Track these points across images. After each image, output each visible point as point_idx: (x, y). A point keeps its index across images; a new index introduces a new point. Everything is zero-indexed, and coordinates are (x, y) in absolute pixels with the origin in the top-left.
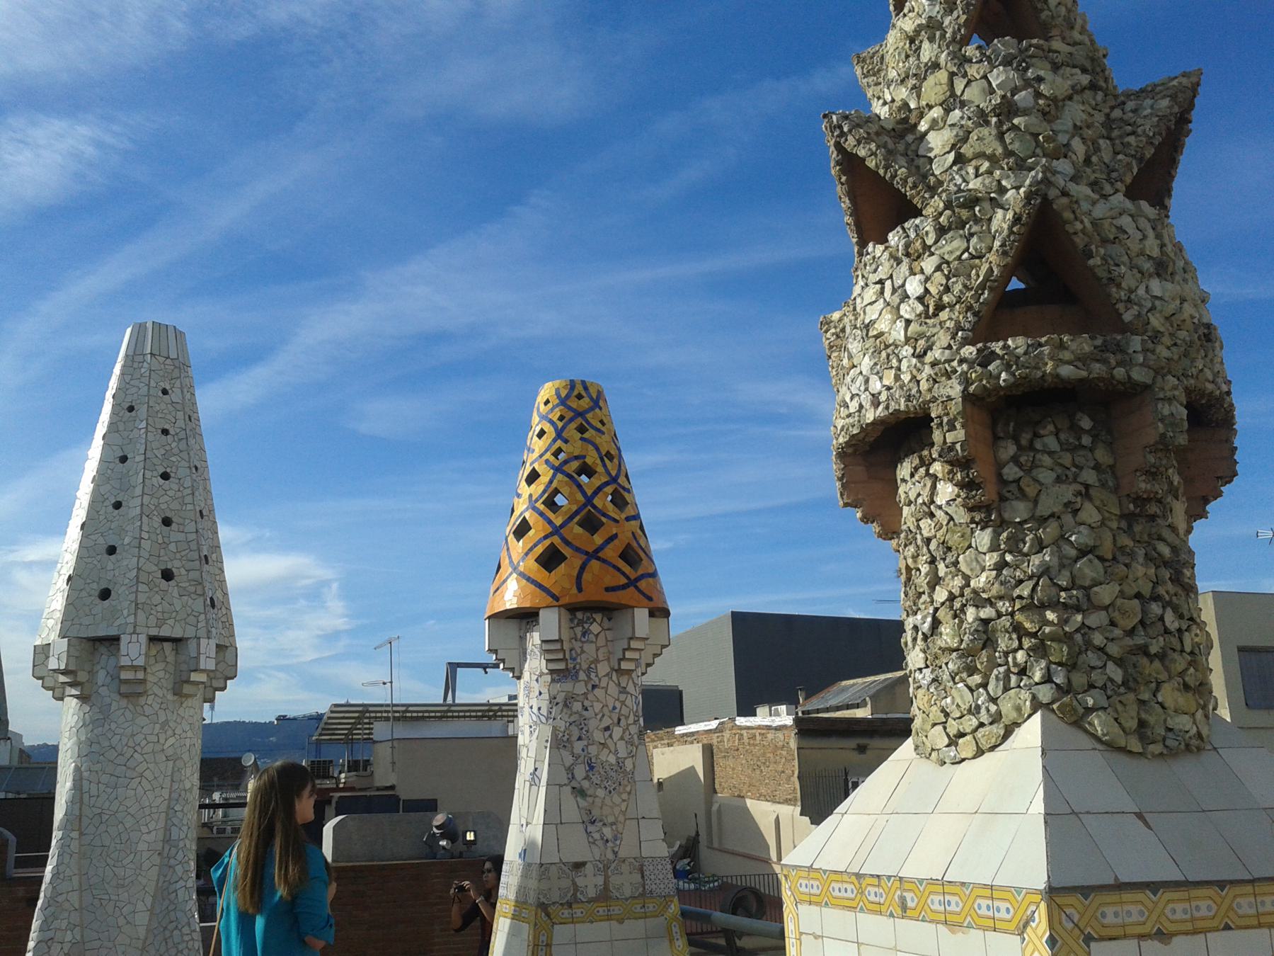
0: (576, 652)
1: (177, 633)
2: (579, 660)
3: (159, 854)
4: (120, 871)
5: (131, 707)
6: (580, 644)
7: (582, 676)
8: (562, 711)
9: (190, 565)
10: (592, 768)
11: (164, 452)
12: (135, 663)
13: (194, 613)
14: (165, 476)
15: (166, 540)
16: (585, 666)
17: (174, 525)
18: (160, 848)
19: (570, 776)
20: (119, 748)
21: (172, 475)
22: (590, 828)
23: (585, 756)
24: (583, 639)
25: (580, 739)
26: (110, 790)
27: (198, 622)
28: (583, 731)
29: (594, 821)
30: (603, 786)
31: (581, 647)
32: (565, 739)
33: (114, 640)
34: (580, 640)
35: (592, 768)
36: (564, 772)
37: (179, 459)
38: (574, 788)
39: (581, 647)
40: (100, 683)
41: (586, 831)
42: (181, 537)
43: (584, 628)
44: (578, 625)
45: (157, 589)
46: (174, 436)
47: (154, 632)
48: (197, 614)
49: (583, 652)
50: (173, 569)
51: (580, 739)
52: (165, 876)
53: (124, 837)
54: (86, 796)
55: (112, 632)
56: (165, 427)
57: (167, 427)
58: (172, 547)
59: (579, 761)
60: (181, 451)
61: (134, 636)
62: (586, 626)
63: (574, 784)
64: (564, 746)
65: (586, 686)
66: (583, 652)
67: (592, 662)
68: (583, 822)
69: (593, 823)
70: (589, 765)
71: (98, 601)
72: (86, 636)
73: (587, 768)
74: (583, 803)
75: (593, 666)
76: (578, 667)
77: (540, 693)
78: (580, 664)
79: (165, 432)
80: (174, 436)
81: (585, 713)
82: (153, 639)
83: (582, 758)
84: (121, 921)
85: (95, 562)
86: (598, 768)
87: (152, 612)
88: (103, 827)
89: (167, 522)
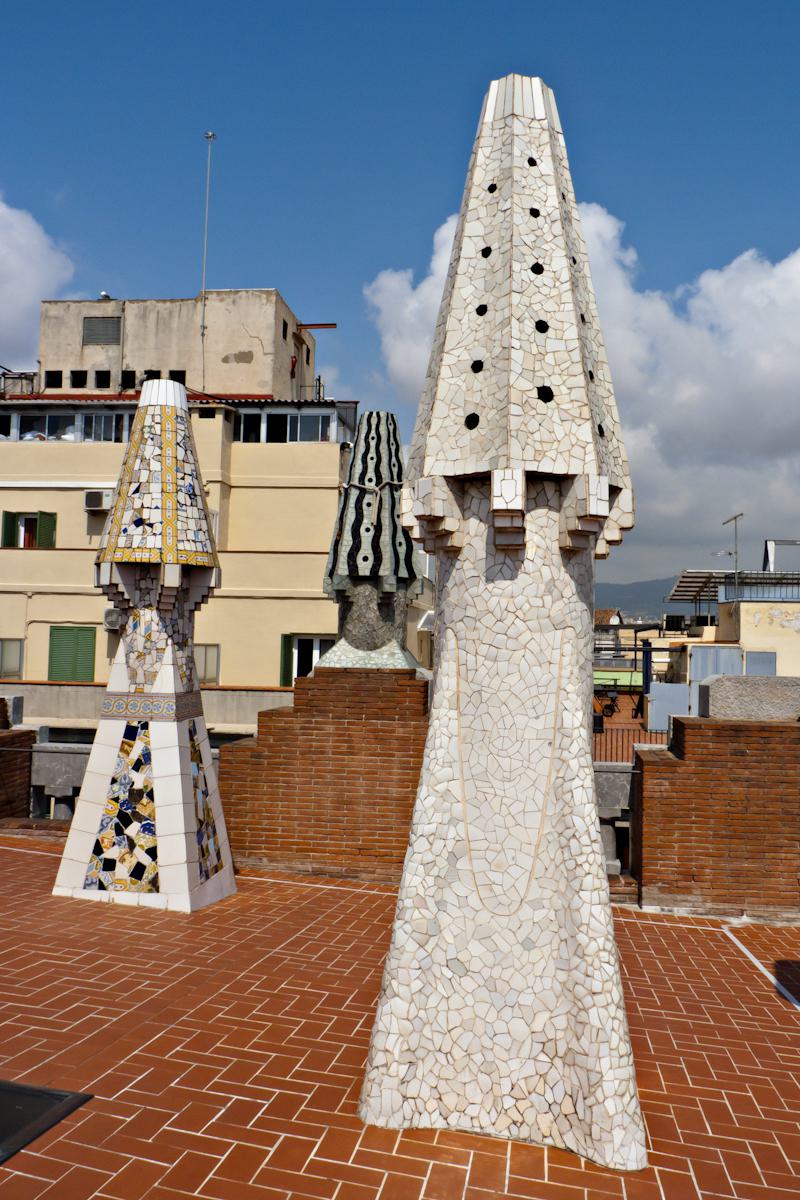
1: (559, 469)
3: (550, 743)
4: (505, 763)
5: (508, 561)
9: (571, 382)
11: (534, 238)
12: (512, 506)
13: (579, 443)
14: (537, 269)
15: (542, 350)
17: (550, 331)
18: (552, 738)
20: (498, 613)
21: (545, 267)
26: (489, 663)
27: (585, 454)
33: (483, 480)
37: (554, 247)
40: (472, 533)
42: (561, 346)
45: (533, 412)
46: (545, 217)
47: (532, 467)
48: (583, 445)
50: (553, 388)
52: (558, 771)
53: (509, 720)
54: (463, 668)
55: (483, 468)
56: (534, 207)
57: (536, 206)
58: (549, 359)
60: (555, 237)
61: (508, 472)
71: (465, 429)
72: (452, 474)
79: (535, 213)
80: (545, 217)
82: (533, 479)
84: (510, 822)
85: (459, 383)
87: (529, 441)
88: (483, 708)
89: (542, 327)
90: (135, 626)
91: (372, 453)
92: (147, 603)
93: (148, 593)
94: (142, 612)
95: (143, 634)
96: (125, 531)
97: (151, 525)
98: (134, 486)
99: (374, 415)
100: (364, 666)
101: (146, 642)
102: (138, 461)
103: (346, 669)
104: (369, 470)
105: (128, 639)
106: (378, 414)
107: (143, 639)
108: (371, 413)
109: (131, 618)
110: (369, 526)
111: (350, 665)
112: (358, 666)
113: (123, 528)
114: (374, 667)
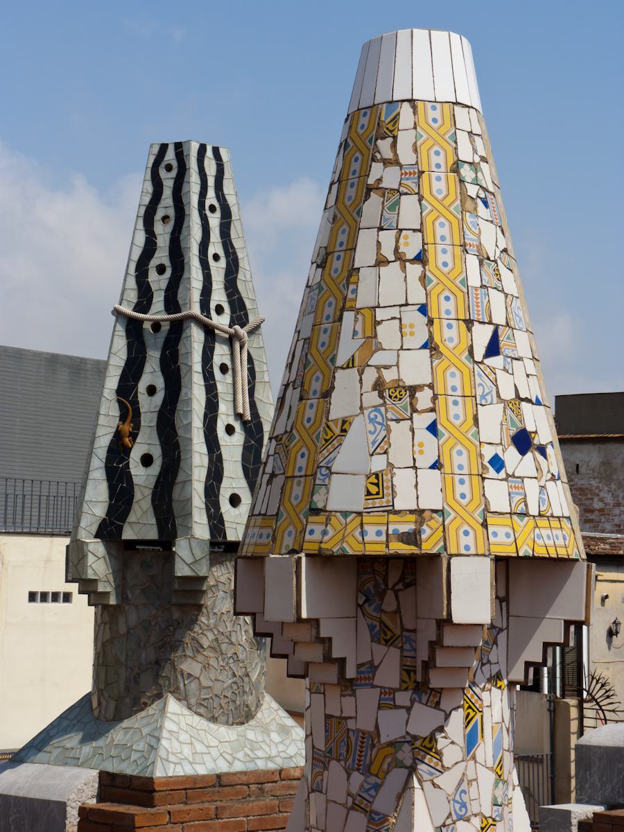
90: (471, 741)
91: (215, 247)
92: (495, 670)
93: (495, 642)
94: (485, 695)
95: (490, 764)
96: (497, 463)
97: (542, 450)
98: (482, 336)
99: (209, 153)
100: (251, 767)
101: (496, 785)
102: (473, 262)
103: (219, 776)
104: (215, 286)
105: (448, 781)
106: (216, 151)
107: (493, 776)
108: (202, 149)
109: (457, 717)
110: (232, 421)
111: (223, 767)
112: (238, 767)
113: (488, 453)
114: (271, 766)
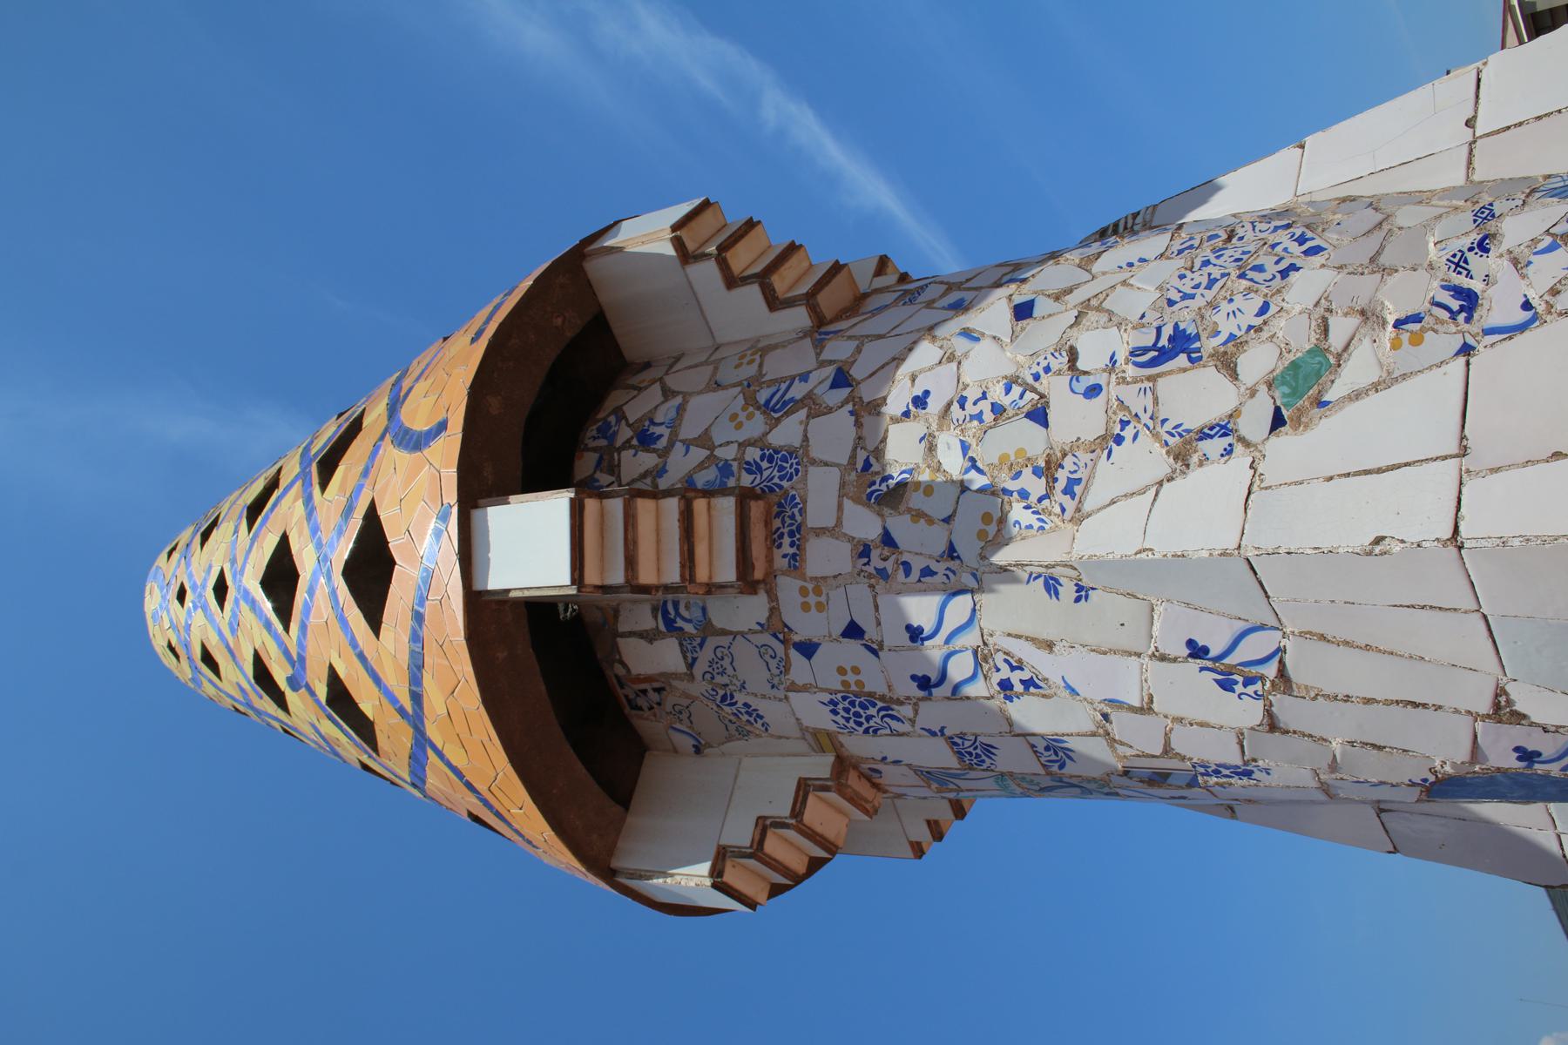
0: (701, 466)
2: (728, 453)
6: (679, 447)
7: (787, 433)
8: (918, 515)
10: (1182, 342)
16: (756, 425)
19: (1215, 446)
22: (1500, 307)
23: (1123, 381)
24: (662, 443)
25: (1039, 415)
28: (1006, 401)
29: (1458, 292)
30: (1278, 281)
31: (688, 444)
32: (1037, 487)
34: (664, 453)
35: (1182, 342)
36: (1196, 475)
38: (1278, 421)
39: (688, 444)
41: (1522, 328)
43: (627, 445)
44: (614, 469)
49: (704, 440)
51: (1039, 415)
59: (1138, 402)
62: (625, 433)
63: (1254, 421)
64: (1068, 491)
65: (830, 410)
66: (704, 440)
67: (750, 401)
68: (1466, 350)
69: (1469, 301)
70: (1163, 356)
73: (1182, 360)
74: (1358, 369)
75: (763, 396)
76: (753, 454)
77: (853, 631)
78: (743, 445)
81: (935, 405)
83: (1130, 395)
86: (1185, 317)
